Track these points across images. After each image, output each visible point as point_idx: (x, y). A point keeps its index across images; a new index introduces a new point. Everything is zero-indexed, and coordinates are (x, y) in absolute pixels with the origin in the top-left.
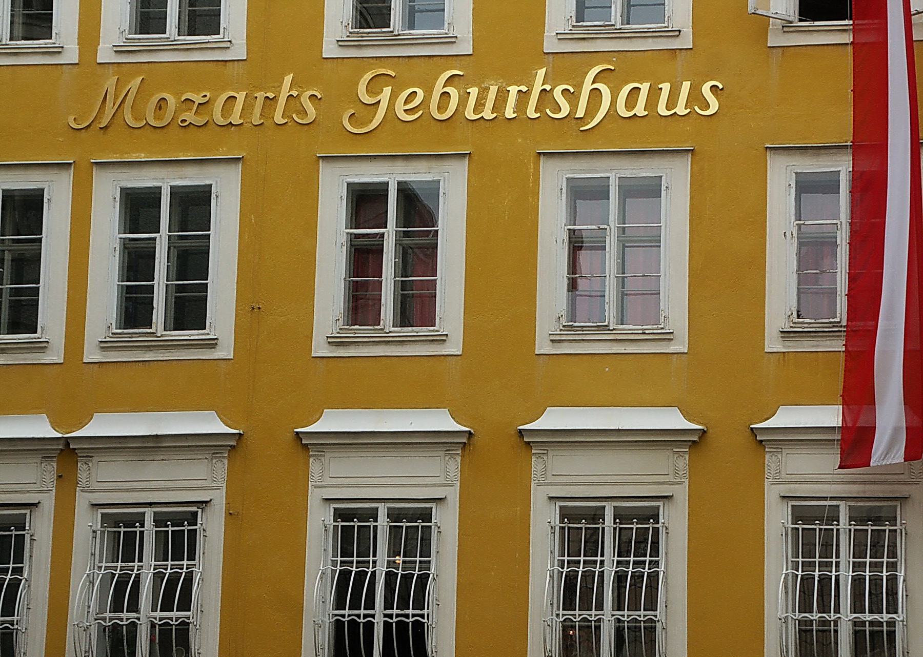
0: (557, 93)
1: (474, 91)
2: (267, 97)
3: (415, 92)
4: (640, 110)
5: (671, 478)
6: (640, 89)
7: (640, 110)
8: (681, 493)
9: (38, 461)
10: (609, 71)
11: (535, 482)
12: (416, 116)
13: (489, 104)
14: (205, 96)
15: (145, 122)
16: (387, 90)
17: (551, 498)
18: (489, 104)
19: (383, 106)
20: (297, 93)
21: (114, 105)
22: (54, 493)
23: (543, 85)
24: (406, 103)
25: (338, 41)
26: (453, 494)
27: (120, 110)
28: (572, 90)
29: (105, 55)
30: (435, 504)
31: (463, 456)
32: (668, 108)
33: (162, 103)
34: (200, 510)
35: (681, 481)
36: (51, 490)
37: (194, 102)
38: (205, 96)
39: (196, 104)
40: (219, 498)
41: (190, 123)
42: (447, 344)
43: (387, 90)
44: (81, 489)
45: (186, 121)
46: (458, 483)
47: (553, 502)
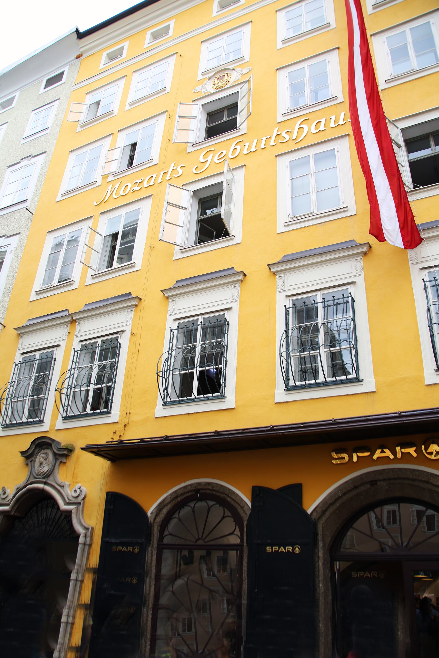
0: (284, 134)
1: (247, 145)
3: (223, 152)
4: (322, 128)
5: (354, 274)
7: (322, 128)
8: (360, 280)
9: (63, 328)
11: (279, 291)
16: (211, 155)
17: (288, 296)
22: (66, 340)
23: (277, 133)
24: (218, 157)
25: (192, 145)
26: (235, 306)
27: (112, 194)
30: (227, 312)
31: (241, 287)
32: (334, 124)
33: (126, 188)
34: (120, 336)
35: (360, 274)
36: (65, 339)
40: (128, 329)
42: (235, 240)
43: (211, 155)
44: (76, 336)
45: (133, 190)
46: (238, 300)
47: (288, 299)
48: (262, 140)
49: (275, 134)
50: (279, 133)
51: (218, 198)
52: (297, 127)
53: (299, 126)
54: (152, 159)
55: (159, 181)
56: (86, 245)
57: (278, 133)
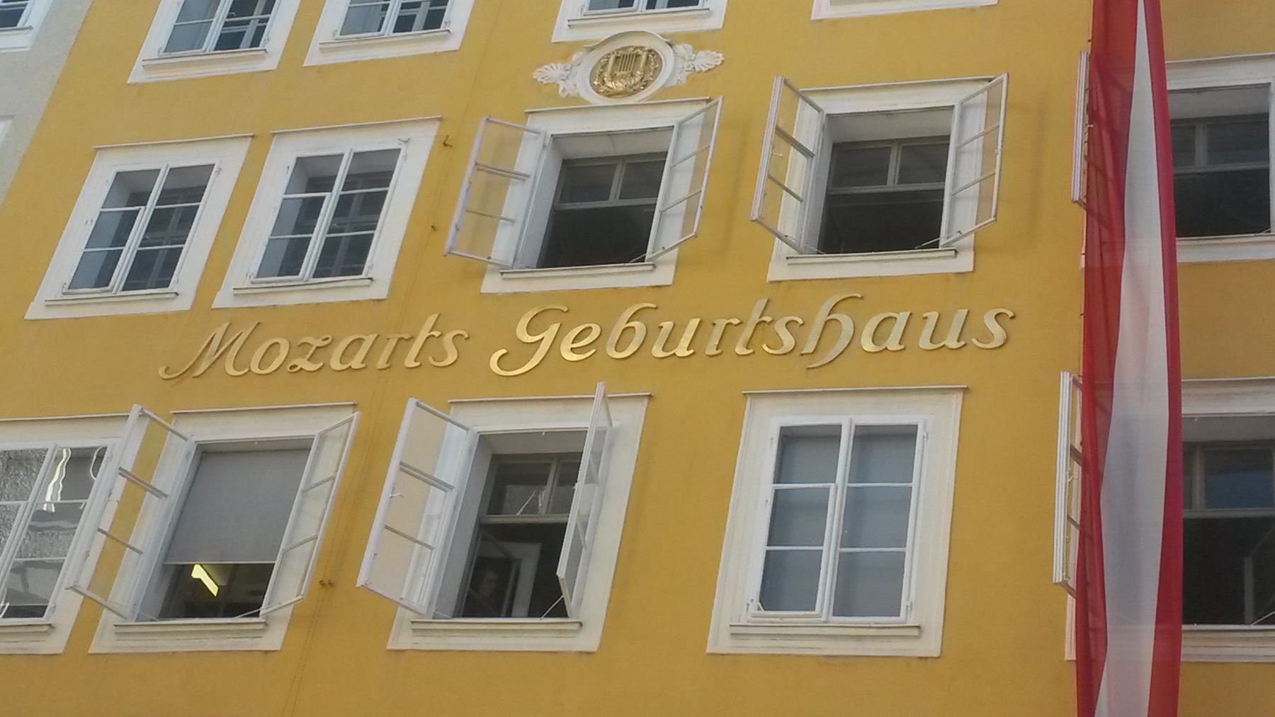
1: (667, 325)
2: (401, 339)
6: (896, 318)
10: (850, 303)
12: (582, 357)
13: (685, 342)
14: (327, 339)
15: (247, 370)
18: (685, 342)
19: (544, 347)
20: (439, 333)
21: (217, 351)
27: (223, 357)
28: (800, 321)
29: (223, 299)
37: (312, 346)
38: (327, 339)
39: (314, 348)
41: (301, 369)
45: (295, 366)
48: (714, 324)
49: (755, 317)
50: (768, 319)
51: (549, 465)
52: (822, 317)
53: (829, 315)
54: (370, 279)
55: (381, 363)
56: (99, 530)
57: (761, 319)
